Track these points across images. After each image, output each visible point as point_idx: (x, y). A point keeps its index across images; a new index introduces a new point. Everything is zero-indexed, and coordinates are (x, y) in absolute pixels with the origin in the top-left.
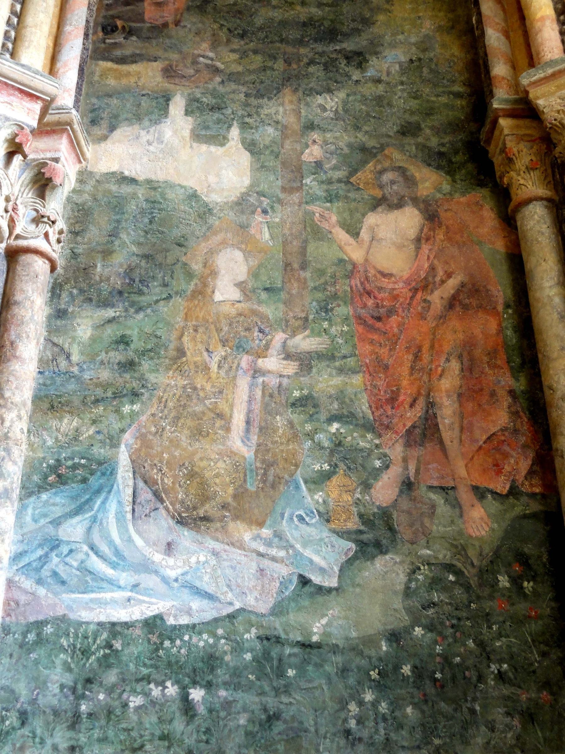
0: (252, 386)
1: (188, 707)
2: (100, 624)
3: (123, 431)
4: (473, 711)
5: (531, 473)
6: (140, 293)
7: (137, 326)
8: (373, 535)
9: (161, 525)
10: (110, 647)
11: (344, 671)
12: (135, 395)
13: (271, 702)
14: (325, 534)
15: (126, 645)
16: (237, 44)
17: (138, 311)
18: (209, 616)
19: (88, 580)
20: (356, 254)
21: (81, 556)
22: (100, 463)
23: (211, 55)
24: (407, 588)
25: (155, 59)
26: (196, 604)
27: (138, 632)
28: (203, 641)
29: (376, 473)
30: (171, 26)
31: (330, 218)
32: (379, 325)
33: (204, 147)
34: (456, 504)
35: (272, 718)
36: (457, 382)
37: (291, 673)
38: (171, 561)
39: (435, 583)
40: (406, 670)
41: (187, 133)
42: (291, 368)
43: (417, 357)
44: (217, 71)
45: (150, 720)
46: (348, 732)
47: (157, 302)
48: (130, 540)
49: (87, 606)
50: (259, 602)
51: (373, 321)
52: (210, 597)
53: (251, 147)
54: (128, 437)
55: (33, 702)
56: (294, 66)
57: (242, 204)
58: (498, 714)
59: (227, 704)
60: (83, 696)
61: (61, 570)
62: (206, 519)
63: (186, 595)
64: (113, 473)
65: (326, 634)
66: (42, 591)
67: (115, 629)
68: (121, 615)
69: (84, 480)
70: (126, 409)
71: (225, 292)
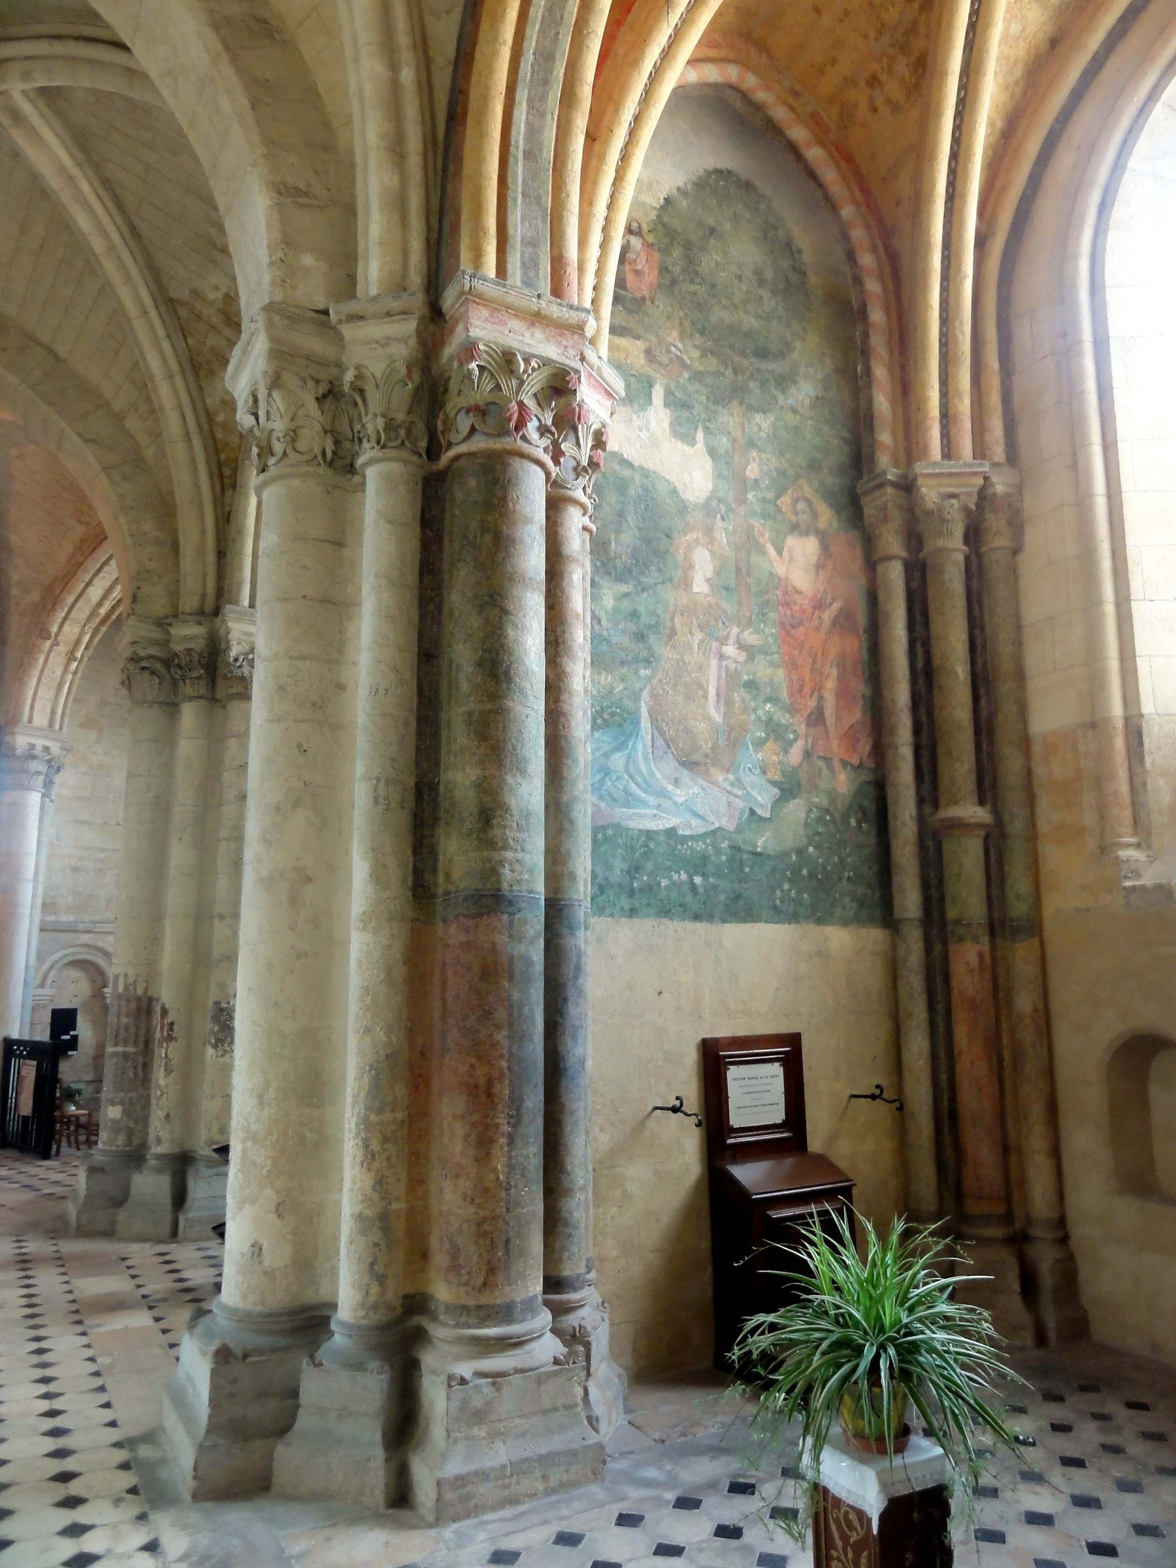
0: (720, 667)
1: (693, 887)
2: (640, 831)
3: (641, 690)
4: (835, 898)
5: (870, 753)
6: (643, 573)
7: (644, 603)
8: (788, 788)
9: (670, 765)
10: (647, 846)
11: (774, 870)
12: (647, 662)
13: (737, 886)
14: (764, 782)
15: (656, 846)
16: (699, 339)
17: (643, 590)
18: (702, 830)
19: (629, 800)
20: (781, 570)
21: (624, 782)
22: (630, 714)
23: (680, 345)
24: (806, 822)
25: (638, 337)
26: (694, 822)
27: (662, 838)
28: (700, 846)
29: (791, 743)
30: (648, 303)
31: (764, 531)
32: (793, 632)
33: (679, 444)
34: (831, 769)
35: (738, 896)
36: (836, 684)
37: (747, 870)
38: (678, 792)
39: (820, 820)
40: (805, 872)
41: (666, 426)
42: (742, 657)
43: (814, 662)
44: (684, 365)
45: (674, 895)
46: (775, 907)
47: (656, 584)
48: (653, 774)
49: (631, 818)
50: (728, 823)
51: (788, 629)
52: (702, 818)
53: (712, 452)
54: (645, 694)
55: (606, 879)
56: (740, 378)
57: (708, 507)
58: (847, 900)
59: (715, 887)
60: (635, 878)
61: (613, 790)
62: (697, 764)
63: (688, 816)
64: (638, 723)
65: (764, 847)
66: (603, 805)
67: (649, 835)
68: (652, 826)
69: (621, 725)
70: (642, 672)
71: (700, 586)
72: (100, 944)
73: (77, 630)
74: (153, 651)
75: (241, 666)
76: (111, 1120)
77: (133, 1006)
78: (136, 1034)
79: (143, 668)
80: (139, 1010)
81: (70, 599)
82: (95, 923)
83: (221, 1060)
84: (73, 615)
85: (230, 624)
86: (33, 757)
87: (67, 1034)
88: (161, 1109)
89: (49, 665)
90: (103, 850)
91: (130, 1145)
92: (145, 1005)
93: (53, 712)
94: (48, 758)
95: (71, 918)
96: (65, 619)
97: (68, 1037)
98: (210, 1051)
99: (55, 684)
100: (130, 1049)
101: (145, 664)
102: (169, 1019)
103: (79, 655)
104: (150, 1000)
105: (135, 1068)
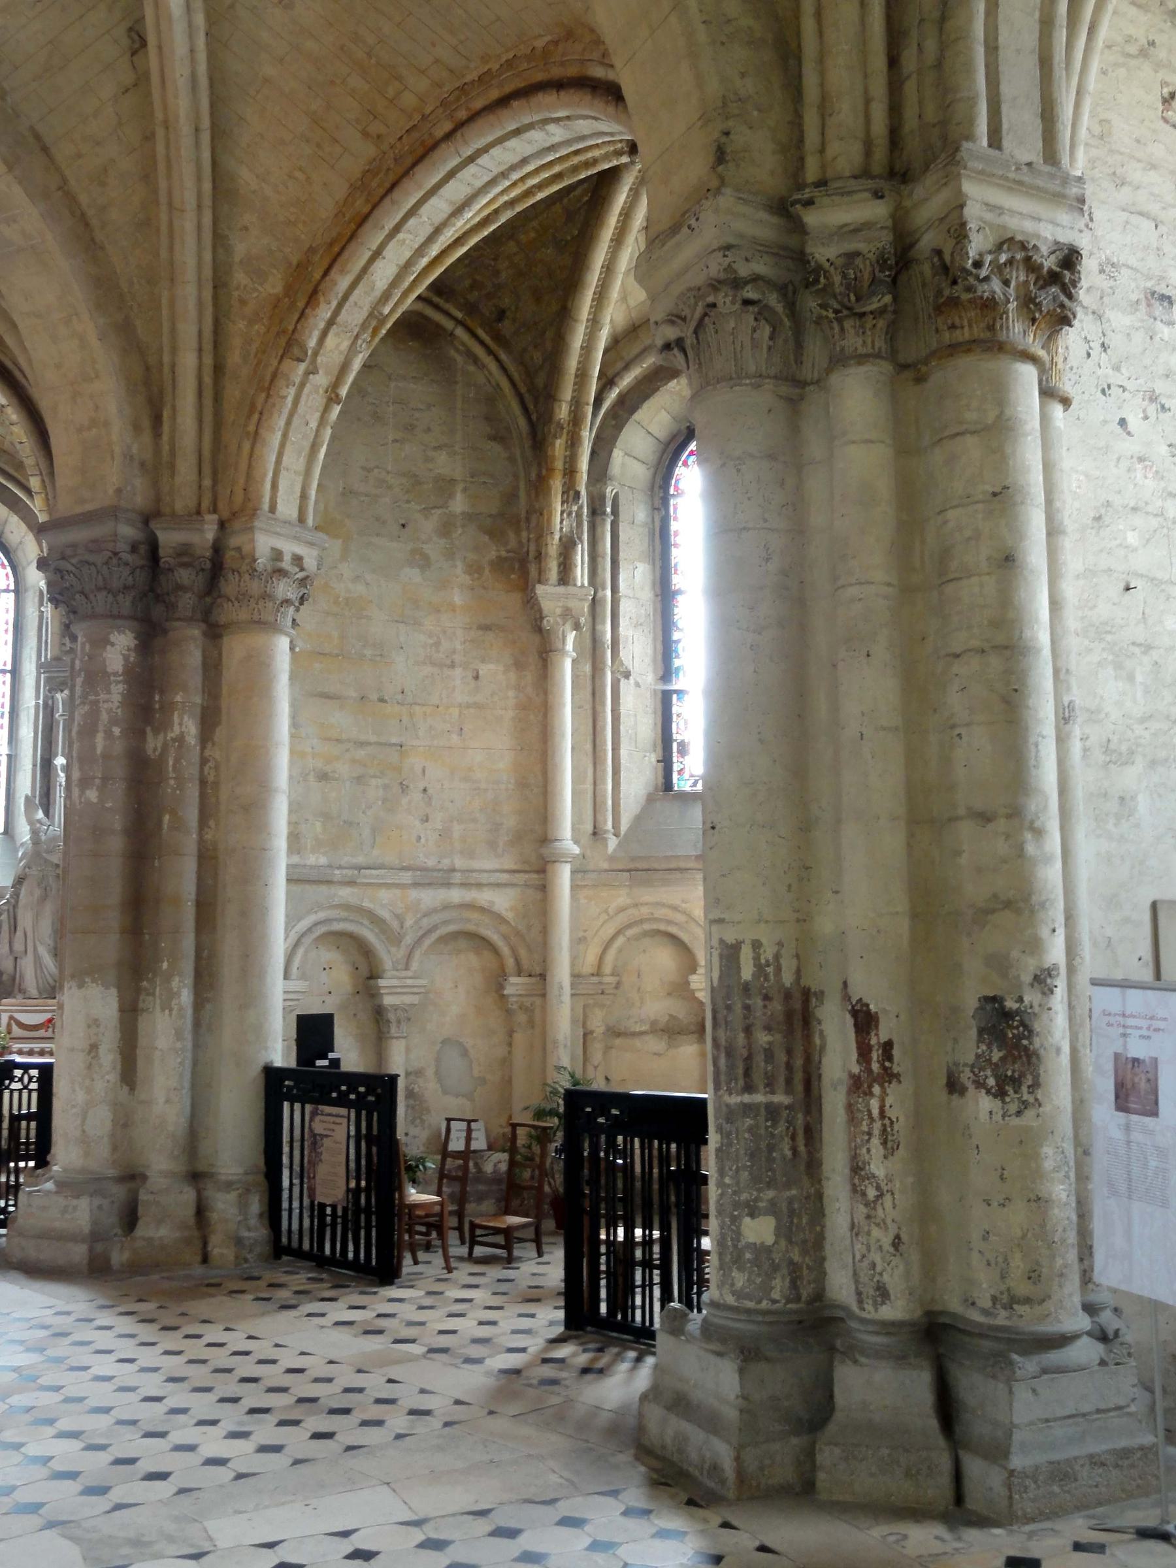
72: (366, 904)
73: (345, 344)
74: (760, 267)
75: (987, 279)
76: (749, 1246)
77: (777, 1006)
78: (789, 1067)
79: (747, 302)
80: (789, 1015)
81: (344, 283)
82: (359, 868)
83: (1015, 1121)
84: (343, 315)
85: (970, 188)
86: (281, 573)
87: (326, 1058)
88: (882, 1225)
89: (301, 408)
90: (362, 744)
91: (798, 1299)
92: (797, 1005)
93: (304, 496)
94: (301, 575)
95: (323, 860)
96: (331, 323)
97: (325, 1063)
98: (985, 1103)
99: (307, 445)
100: (780, 1098)
101: (750, 293)
102: (884, 1032)
103: (344, 391)
104: (806, 994)
105: (793, 1138)
